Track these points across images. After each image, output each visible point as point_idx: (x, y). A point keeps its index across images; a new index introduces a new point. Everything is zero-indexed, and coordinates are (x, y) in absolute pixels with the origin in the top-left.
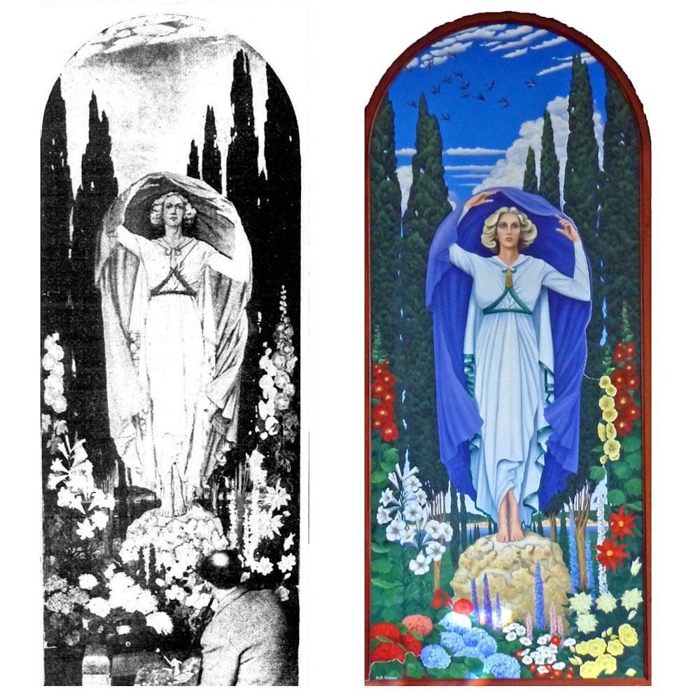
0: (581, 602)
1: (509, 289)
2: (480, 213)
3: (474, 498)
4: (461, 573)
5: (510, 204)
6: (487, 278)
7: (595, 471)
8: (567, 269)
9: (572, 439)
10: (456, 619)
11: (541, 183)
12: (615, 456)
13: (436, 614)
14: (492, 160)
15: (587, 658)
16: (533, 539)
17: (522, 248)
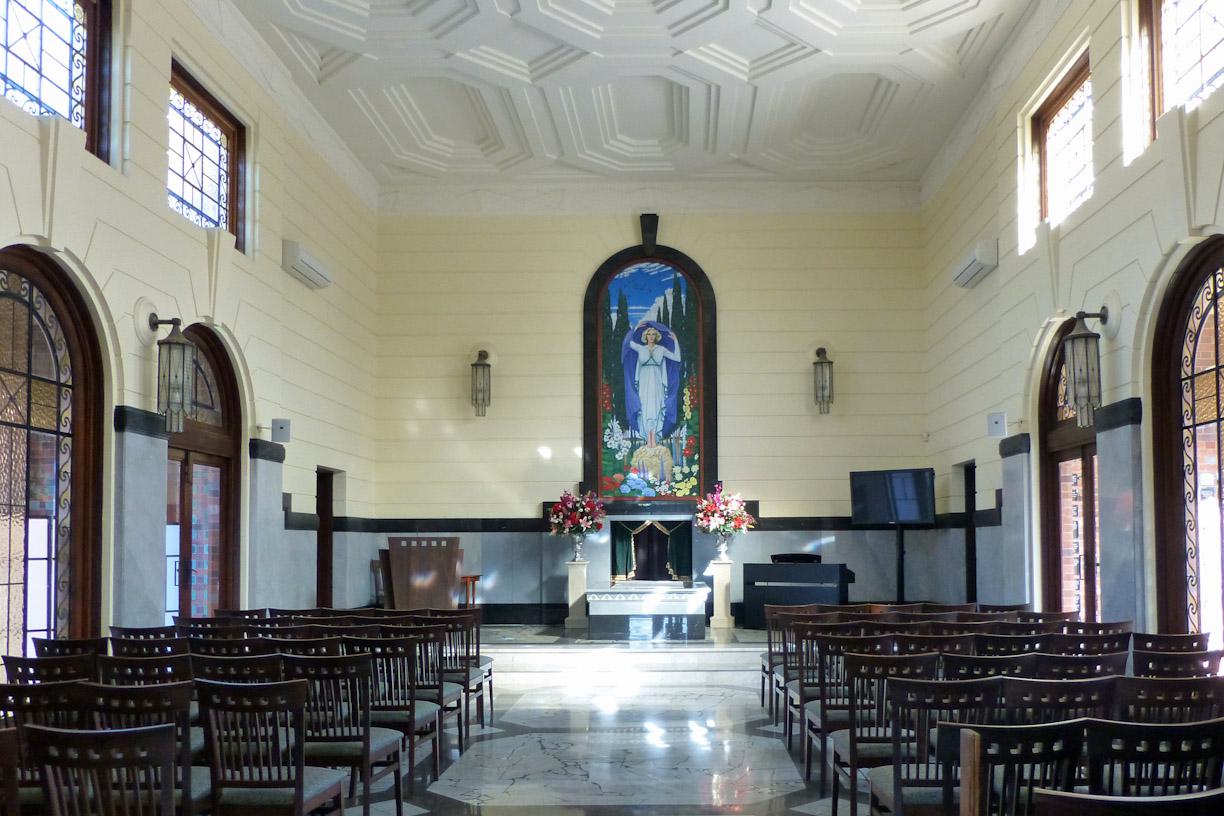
0: (677, 470)
1: (651, 357)
2: (641, 330)
3: (639, 431)
4: (634, 459)
5: (651, 327)
6: (643, 353)
7: (682, 423)
8: (672, 349)
9: (674, 411)
10: (633, 475)
11: (663, 319)
12: (689, 417)
13: (625, 474)
14: (645, 311)
15: (679, 489)
16: (660, 447)
17: (656, 342)
